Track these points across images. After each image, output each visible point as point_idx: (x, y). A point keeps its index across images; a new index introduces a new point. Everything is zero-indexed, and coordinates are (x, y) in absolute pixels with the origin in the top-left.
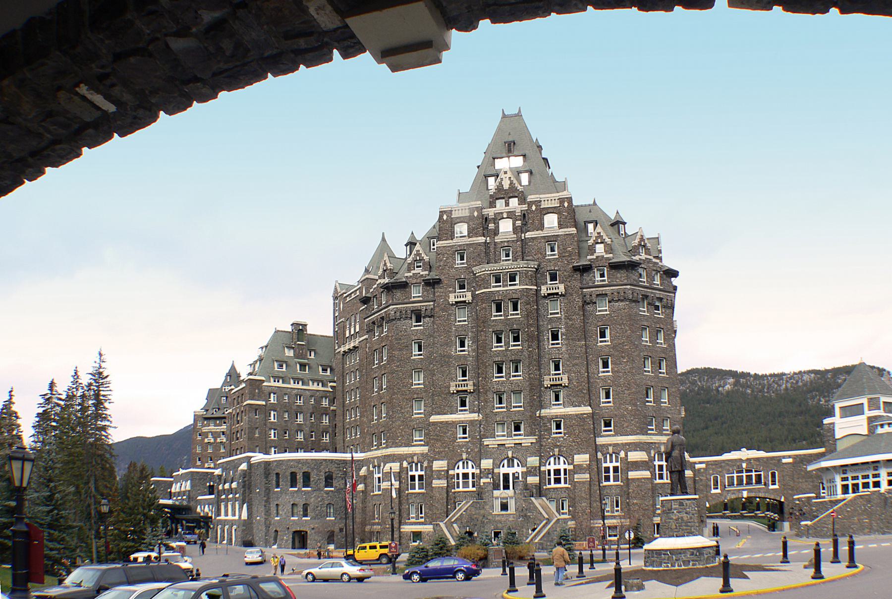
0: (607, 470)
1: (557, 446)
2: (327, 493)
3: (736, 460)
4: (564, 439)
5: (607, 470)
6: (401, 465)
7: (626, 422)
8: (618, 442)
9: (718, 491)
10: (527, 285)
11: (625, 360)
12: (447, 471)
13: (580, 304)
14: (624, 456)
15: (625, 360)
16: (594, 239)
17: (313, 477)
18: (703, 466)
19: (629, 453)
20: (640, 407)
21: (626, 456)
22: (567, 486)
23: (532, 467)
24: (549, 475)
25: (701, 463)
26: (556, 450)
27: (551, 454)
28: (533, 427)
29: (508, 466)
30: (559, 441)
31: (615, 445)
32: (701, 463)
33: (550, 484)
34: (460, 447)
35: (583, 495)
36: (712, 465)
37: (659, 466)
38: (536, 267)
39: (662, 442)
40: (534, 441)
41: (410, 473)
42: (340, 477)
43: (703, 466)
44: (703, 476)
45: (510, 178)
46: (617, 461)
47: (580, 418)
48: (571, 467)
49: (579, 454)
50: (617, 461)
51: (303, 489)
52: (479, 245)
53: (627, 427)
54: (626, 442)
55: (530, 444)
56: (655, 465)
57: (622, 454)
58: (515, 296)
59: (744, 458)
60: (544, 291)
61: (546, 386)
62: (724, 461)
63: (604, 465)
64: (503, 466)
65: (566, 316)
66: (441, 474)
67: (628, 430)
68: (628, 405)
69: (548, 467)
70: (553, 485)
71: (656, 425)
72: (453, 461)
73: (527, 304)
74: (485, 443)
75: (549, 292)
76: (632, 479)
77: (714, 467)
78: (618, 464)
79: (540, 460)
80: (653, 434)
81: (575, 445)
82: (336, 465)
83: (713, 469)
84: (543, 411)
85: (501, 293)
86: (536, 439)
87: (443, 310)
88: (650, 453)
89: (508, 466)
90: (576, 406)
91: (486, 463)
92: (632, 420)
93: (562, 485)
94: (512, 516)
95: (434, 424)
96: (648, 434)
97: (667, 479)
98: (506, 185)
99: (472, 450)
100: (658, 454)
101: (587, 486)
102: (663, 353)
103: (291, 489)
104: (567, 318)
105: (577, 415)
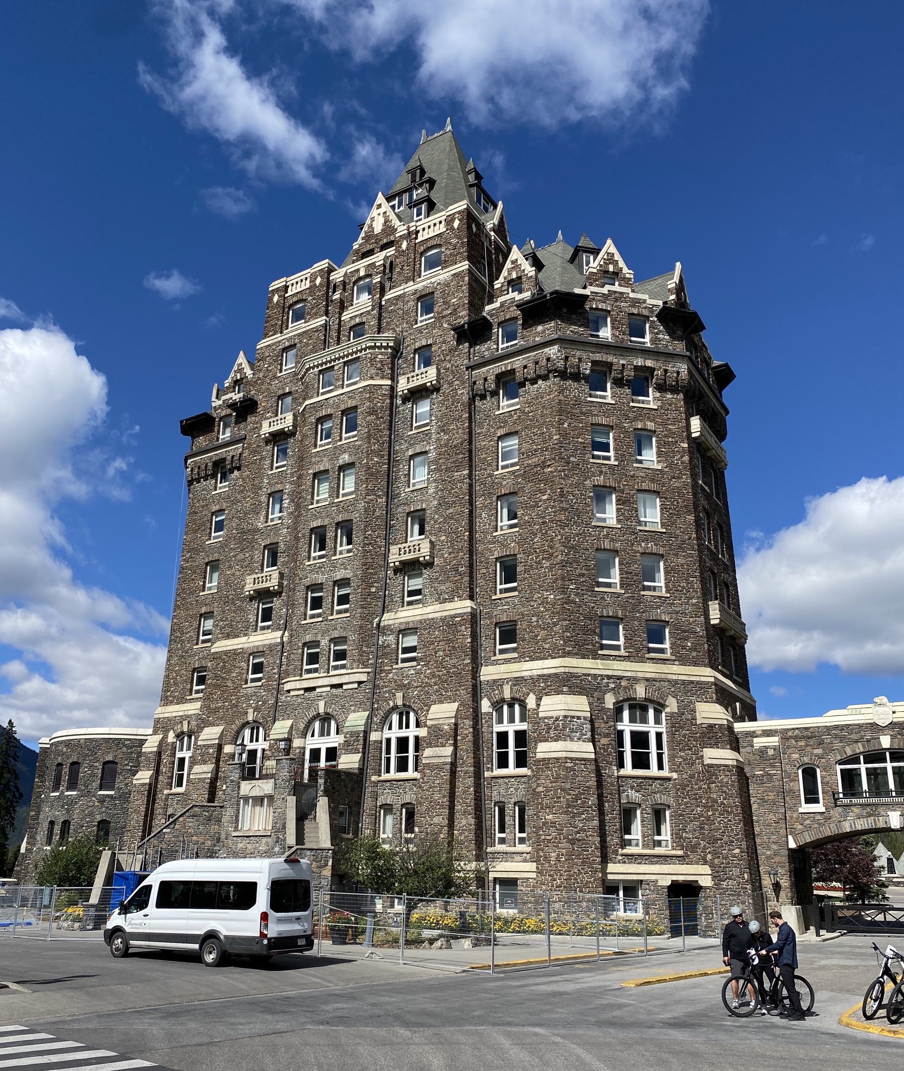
0: (503, 738)
1: (401, 687)
2: (102, 800)
3: (860, 726)
4: (418, 673)
5: (503, 738)
6: (165, 737)
7: (544, 629)
8: (524, 674)
9: (819, 807)
10: (372, 378)
11: (545, 497)
12: (220, 747)
13: (465, 398)
14: (534, 706)
15: (545, 497)
16: (506, 274)
17: (85, 770)
18: (774, 741)
19: (546, 700)
20: (577, 594)
21: (538, 705)
22: (417, 775)
23: (352, 734)
24: (388, 751)
25: (768, 733)
26: (399, 695)
27: (392, 704)
28: (365, 649)
29: (322, 734)
30: (407, 676)
31: (517, 681)
32: (768, 733)
33: (388, 771)
34: (248, 698)
35: (437, 796)
36: (797, 738)
37: (633, 734)
38: (391, 344)
39: (640, 675)
40: (363, 678)
41: (179, 755)
42: (130, 770)
43: (774, 741)
44: (773, 766)
45: (385, 213)
46: (523, 719)
47: (449, 626)
48: (423, 732)
49: (441, 702)
50: (523, 719)
51: (66, 793)
52: (317, 331)
53: (544, 640)
54: (540, 672)
55: (356, 685)
56: (620, 733)
57: (531, 702)
58: (351, 403)
59: (883, 722)
60: (403, 385)
61: (392, 565)
62: (828, 729)
63: (498, 728)
64: (313, 735)
65: (439, 427)
66: (208, 754)
67: (547, 646)
68: (547, 591)
69: (387, 734)
70: (393, 774)
71: (626, 637)
72: (233, 726)
73: (370, 414)
74: (287, 687)
75: (411, 385)
76: (544, 760)
77: (802, 743)
78: (523, 726)
79: (370, 718)
80: (616, 658)
81: (435, 684)
82: (125, 749)
83: (801, 750)
84: (386, 616)
85: (331, 401)
86: (368, 673)
87: (255, 452)
88: (601, 700)
89: (322, 734)
90: (445, 601)
91: (281, 728)
92: (555, 624)
93: (410, 773)
94: (264, 840)
95: (217, 657)
96: (595, 656)
97: (660, 767)
98: (378, 227)
99: (264, 703)
100: (631, 707)
101: (446, 775)
102: (653, 481)
103: (52, 794)
104: (443, 429)
105: (443, 619)
